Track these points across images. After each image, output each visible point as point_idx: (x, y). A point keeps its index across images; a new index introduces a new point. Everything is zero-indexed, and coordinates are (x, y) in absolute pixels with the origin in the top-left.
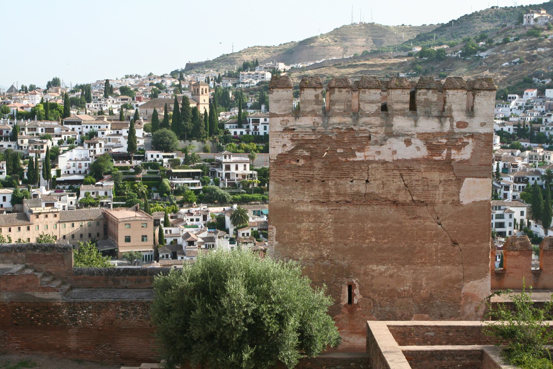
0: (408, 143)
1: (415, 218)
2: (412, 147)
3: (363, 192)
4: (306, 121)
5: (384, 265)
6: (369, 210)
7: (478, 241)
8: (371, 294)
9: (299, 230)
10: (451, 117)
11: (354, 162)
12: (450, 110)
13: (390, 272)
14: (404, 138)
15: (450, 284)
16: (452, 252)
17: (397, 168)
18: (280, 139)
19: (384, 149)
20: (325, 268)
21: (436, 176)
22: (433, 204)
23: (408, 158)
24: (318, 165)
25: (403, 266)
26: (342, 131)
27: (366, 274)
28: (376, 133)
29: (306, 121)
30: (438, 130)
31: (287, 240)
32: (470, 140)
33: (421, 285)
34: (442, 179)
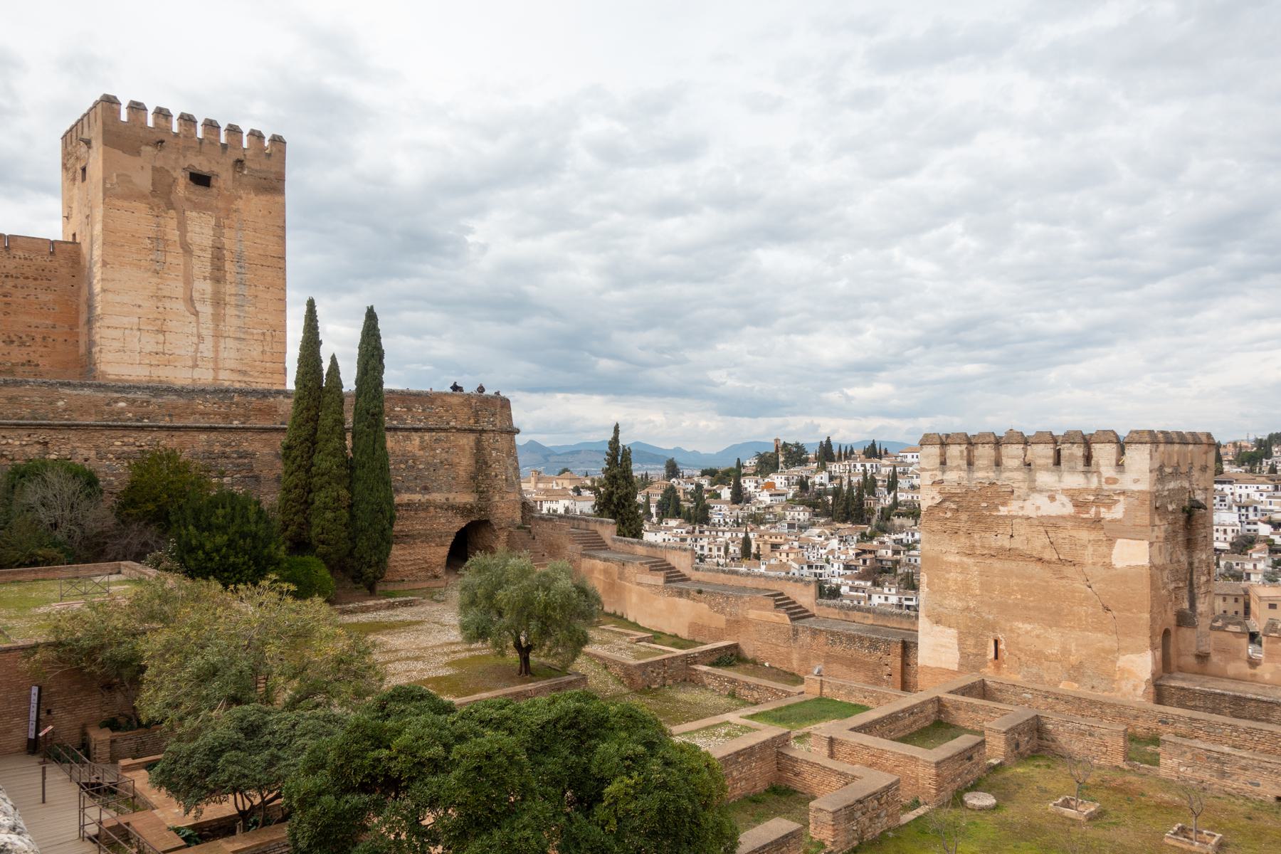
0: (1052, 498)
1: (1062, 578)
2: (1057, 503)
3: (1008, 547)
4: (952, 476)
5: (1029, 623)
6: (1012, 565)
7: (1135, 610)
8: (1017, 652)
9: (948, 579)
10: (1099, 473)
11: (998, 516)
12: (1098, 465)
13: (1037, 632)
14: (1047, 494)
15: (1103, 654)
16: (1104, 619)
17: (1042, 524)
18: (930, 492)
19: (1028, 504)
20: (972, 619)
21: (1084, 535)
22: (1082, 565)
23: (1054, 515)
24: (964, 516)
25: (1051, 627)
26: (986, 485)
27: (1012, 630)
28: (1019, 488)
29: (952, 476)
30: (1085, 486)
31: (937, 588)
32: (1122, 498)
33: (1070, 651)
34: (1091, 539)
